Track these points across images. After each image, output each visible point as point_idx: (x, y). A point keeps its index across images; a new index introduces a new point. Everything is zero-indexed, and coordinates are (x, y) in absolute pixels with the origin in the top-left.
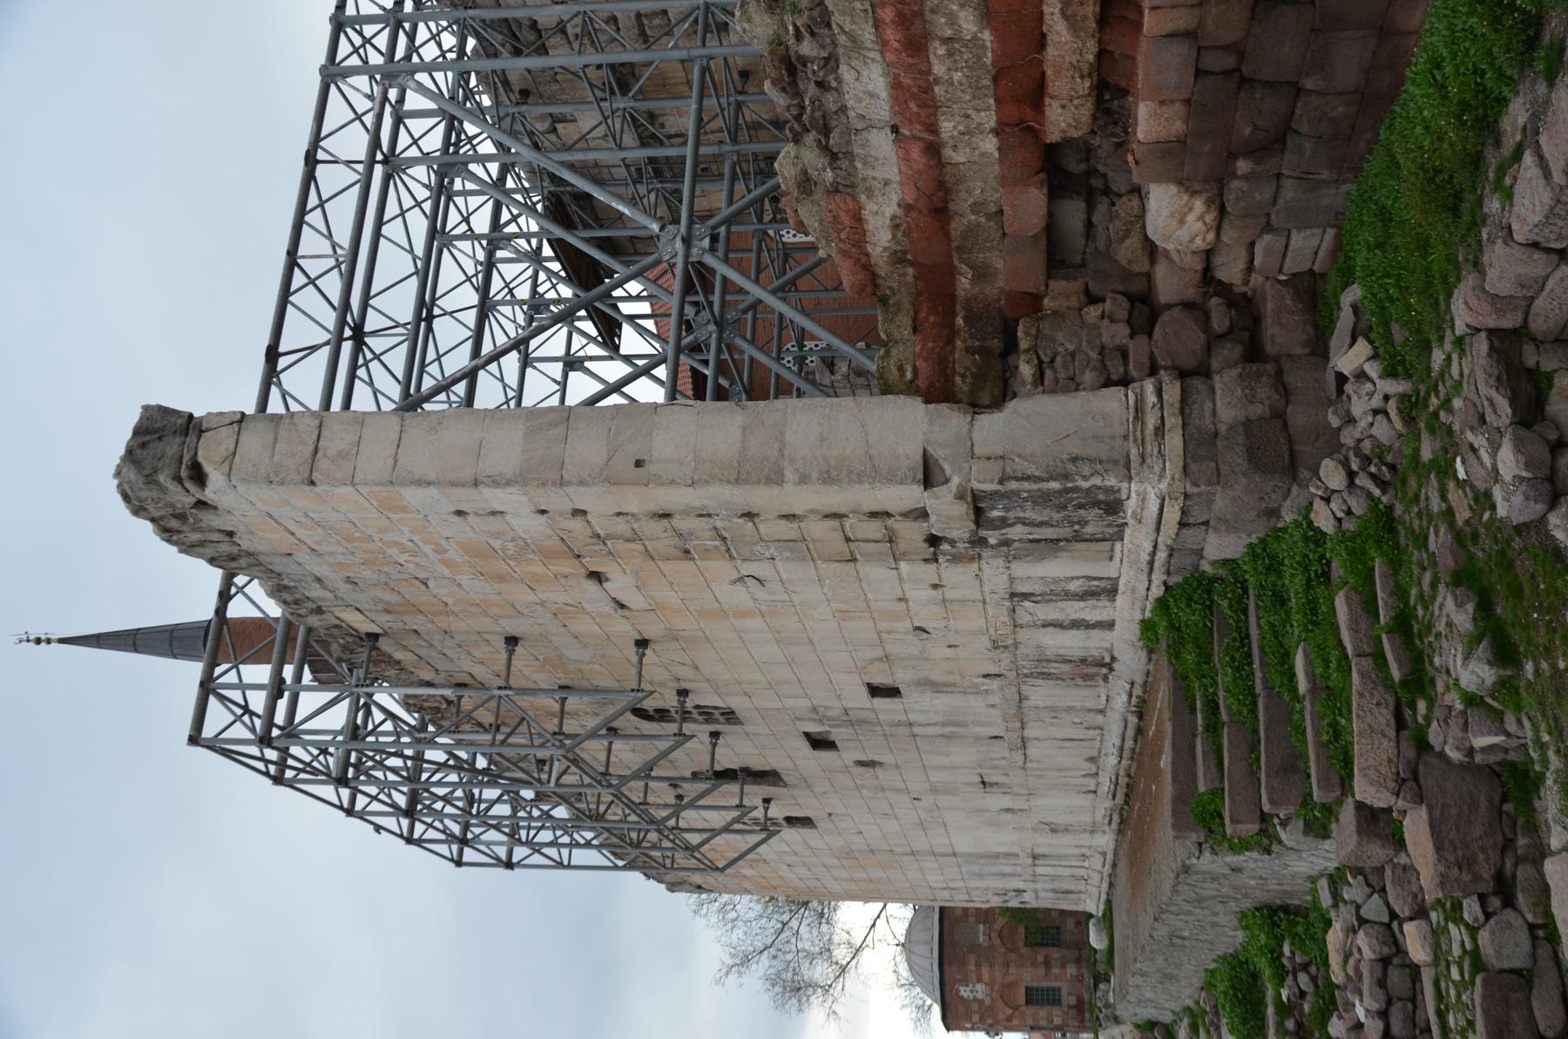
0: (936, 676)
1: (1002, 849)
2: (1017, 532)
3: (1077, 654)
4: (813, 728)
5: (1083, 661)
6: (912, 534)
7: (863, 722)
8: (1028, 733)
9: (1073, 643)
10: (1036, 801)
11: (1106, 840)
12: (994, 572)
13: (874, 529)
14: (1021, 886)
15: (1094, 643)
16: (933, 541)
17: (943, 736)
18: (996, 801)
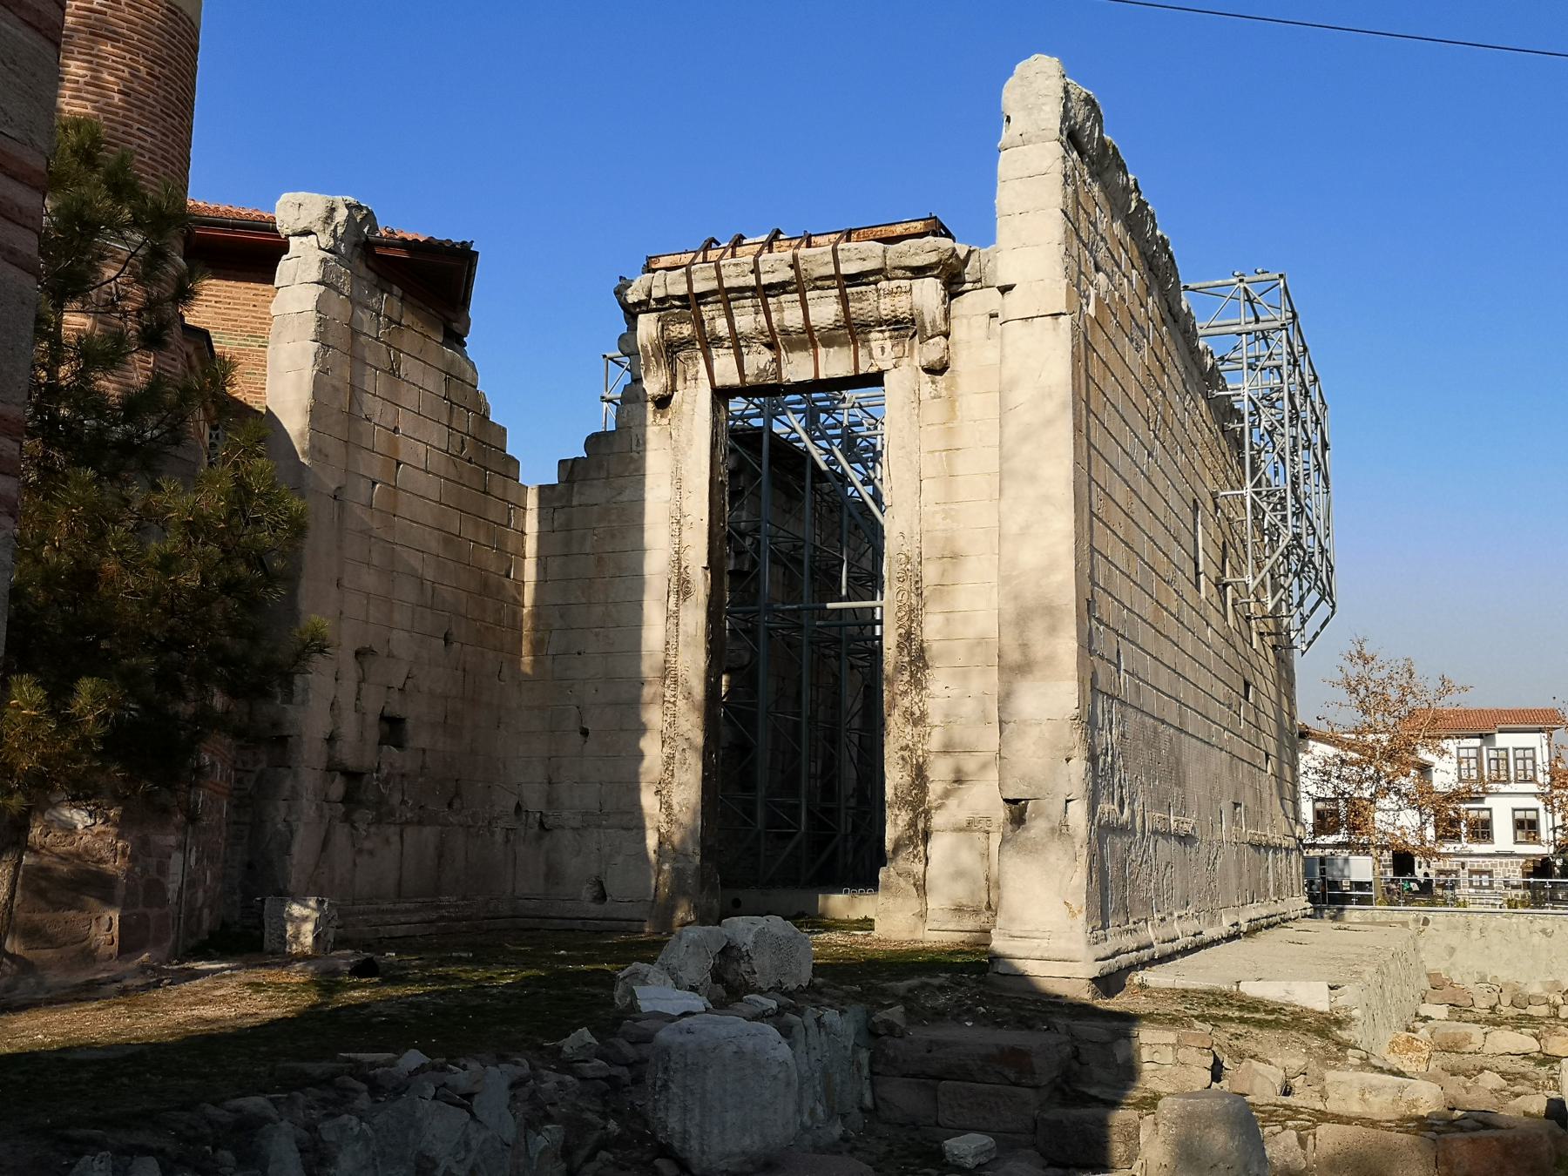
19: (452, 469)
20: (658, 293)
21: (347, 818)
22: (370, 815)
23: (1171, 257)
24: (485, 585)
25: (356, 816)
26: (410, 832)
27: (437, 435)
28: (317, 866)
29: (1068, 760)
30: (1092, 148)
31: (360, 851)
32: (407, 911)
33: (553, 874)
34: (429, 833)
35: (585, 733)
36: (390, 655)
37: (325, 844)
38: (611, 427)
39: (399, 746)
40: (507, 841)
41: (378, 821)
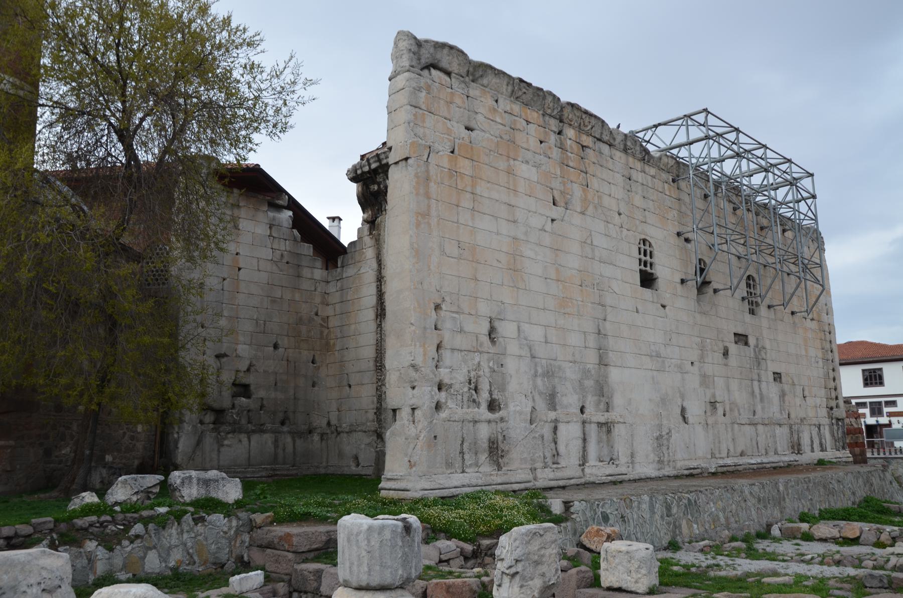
0: (786, 398)
1: (618, 401)
2: (835, 427)
3: (802, 442)
4: (752, 341)
5: (799, 445)
6: (833, 403)
7: (759, 364)
8: (760, 428)
9: (805, 441)
10: (699, 429)
11: (647, 469)
12: (826, 421)
13: (833, 396)
14: (517, 406)
15: (806, 447)
16: (832, 409)
17: (753, 392)
18: (695, 410)
19: (275, 267)
20: (359, 172)
21: (215, 430)
22: (228, 428)
23: (586, 112)
24: (301, 319)
25: (221, 429)
26: (255, 438)
27: (266, 253)
28: (194, 452)
29: (413, 388)
30: (454, 68)
31: (223, 445)
32: (254, 472)
33: (341, 455)
34: (268, 438)
35: (350, 386)
36: (237, 356)
37: (199, 442)
38: (355, 239)
39: (249, 397)
40: (322, 439)
41: (233, 432)
